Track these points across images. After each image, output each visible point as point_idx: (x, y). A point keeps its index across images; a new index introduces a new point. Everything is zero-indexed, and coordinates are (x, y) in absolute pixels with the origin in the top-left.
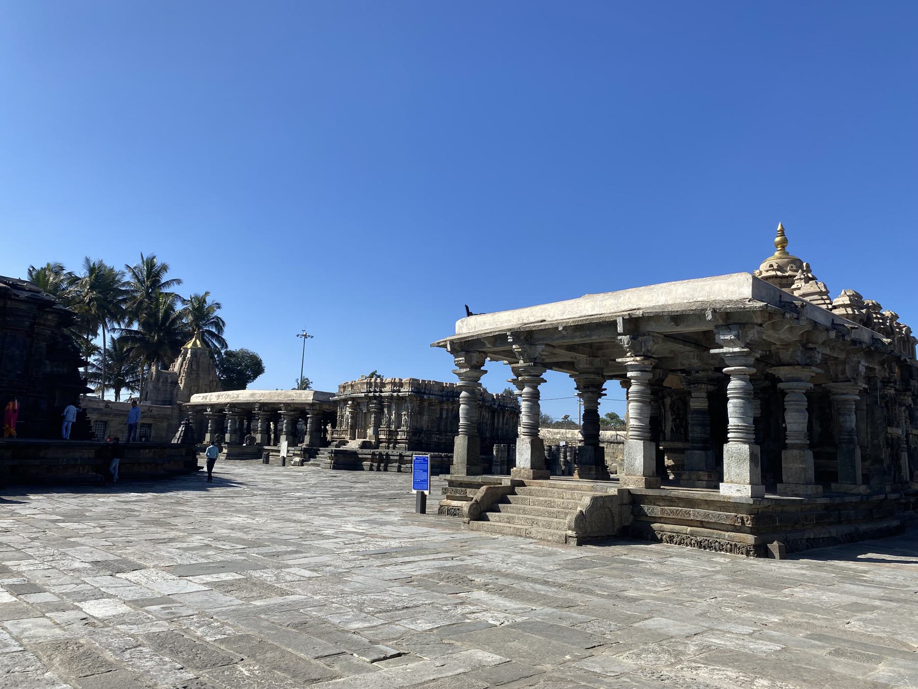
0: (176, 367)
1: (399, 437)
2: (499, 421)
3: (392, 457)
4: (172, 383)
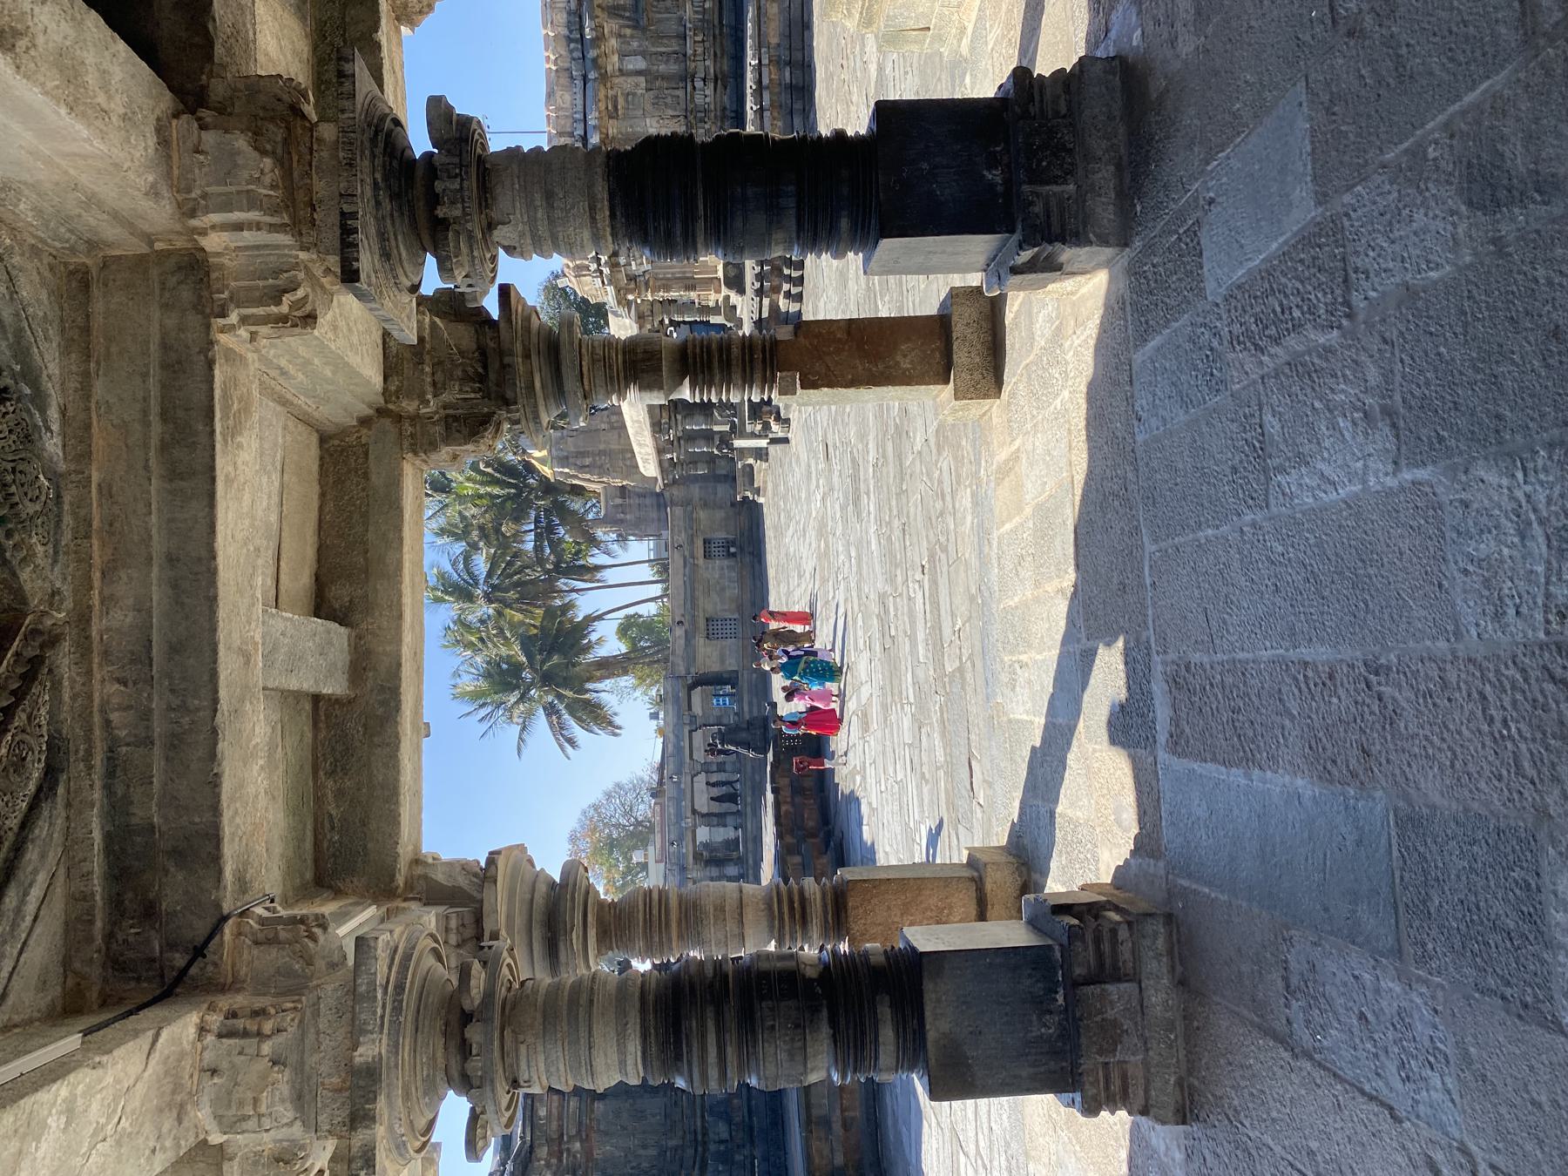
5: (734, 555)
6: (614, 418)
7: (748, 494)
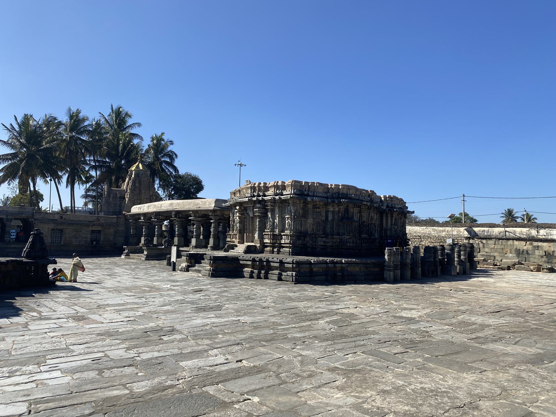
0: (124, 187)
1: (283, 241)
2: (388, 223)
3: (272, 264)
4: (120, 197)
5: (92, 243)
6: (154, 197)
7: (126, 251)
